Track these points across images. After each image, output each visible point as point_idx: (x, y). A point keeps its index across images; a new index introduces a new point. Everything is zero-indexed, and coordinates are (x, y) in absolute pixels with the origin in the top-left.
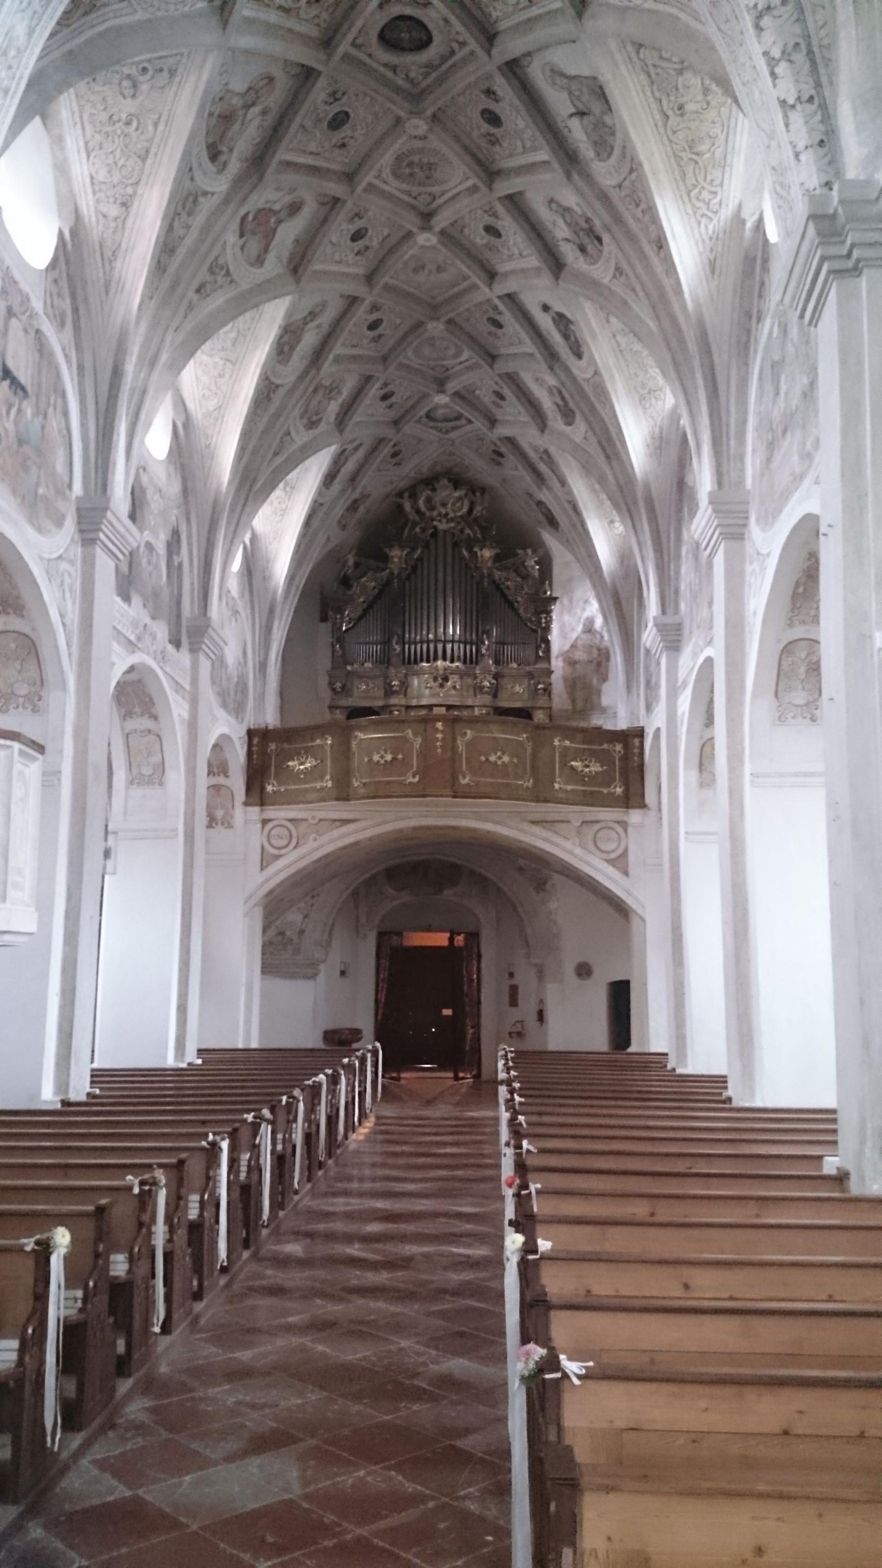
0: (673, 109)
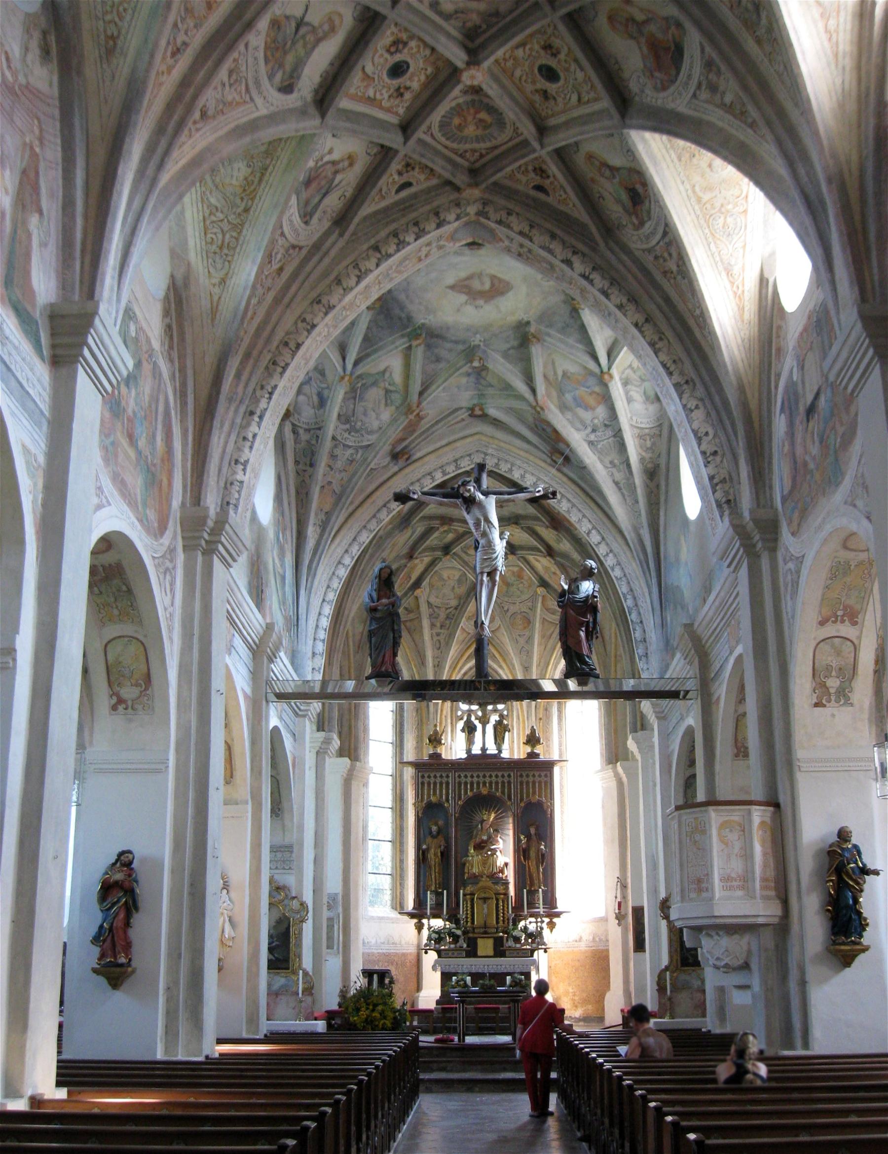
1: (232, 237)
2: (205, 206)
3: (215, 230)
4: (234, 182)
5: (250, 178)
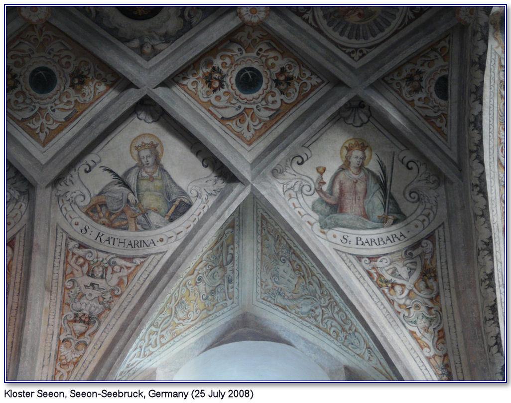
0: (199, 273)
1: (338, 313)
2: (309, 320)
3: (329, 326)
4: (294, 282)
5: (295, 265)
